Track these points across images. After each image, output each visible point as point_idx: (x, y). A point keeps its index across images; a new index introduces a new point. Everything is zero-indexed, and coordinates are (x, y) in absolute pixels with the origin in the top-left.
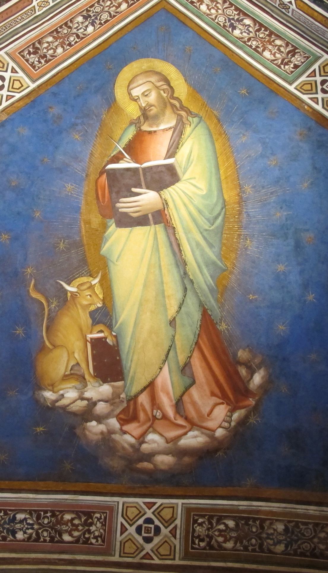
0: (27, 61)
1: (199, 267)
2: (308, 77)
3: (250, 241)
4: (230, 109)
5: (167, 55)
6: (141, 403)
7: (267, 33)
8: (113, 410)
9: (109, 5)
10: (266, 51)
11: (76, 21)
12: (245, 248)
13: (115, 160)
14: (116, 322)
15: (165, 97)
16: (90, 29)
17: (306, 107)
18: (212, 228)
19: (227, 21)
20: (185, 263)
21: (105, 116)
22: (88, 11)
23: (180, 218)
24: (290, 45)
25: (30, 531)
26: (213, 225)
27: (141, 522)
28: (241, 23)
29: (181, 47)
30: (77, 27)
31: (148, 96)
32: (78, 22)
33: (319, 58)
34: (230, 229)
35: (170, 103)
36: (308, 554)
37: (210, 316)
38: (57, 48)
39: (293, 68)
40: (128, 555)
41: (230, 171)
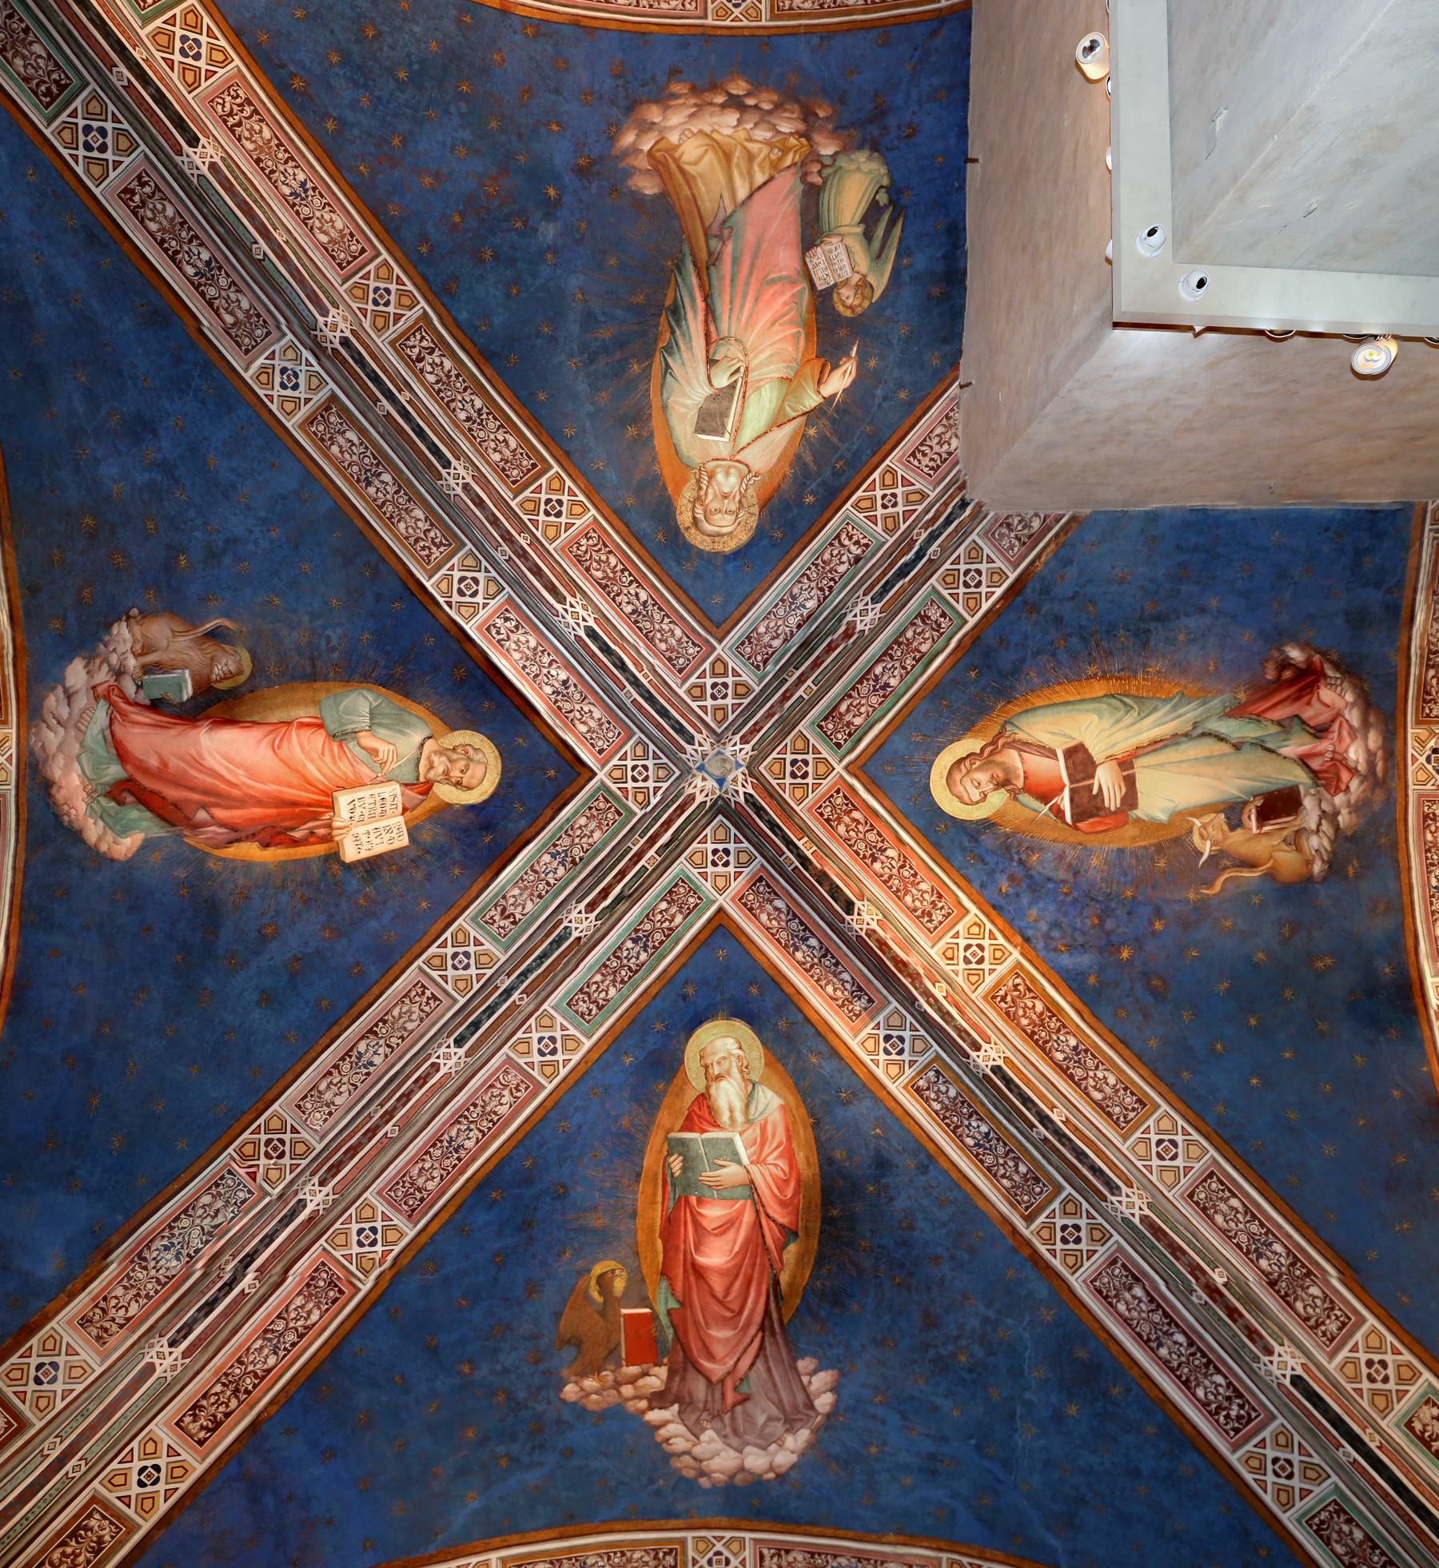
16: (891, 853)
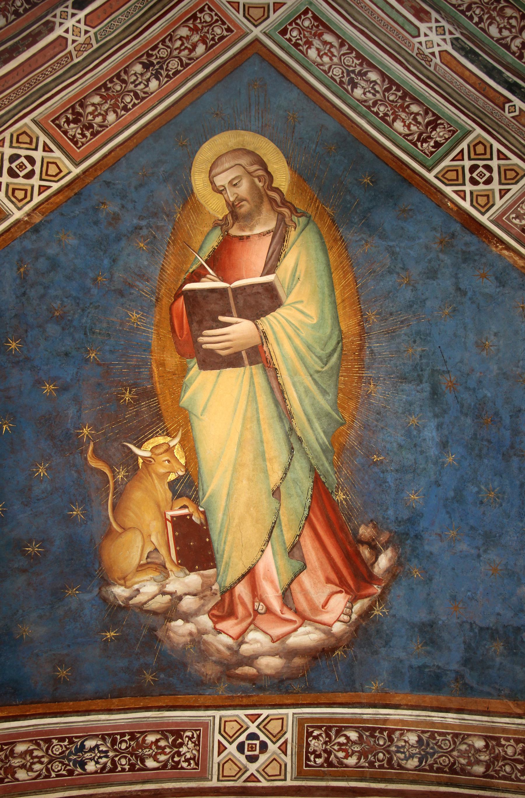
0: (65, 133)
1: (309, 420)
2: (453, 160)
3: (374, 385)
4: (349, 206)
5: (262, 126)
6: (239, 595)
7: (399, 94)
8: (203, 605)
9: (179, 46)
10: (397, 121)
11: (133, 72)
12: (367, 395)
13: (195, 277)
14: (204, 495)
15: (261, 188)
16: (154, 84)
17: (449, 204)
18: (326, 368)
19: (345, 75)
20: (290, 415)
21: (179, 215)
22: (149, 56)
23: (283, 356)
24: (430, 113)
25: (104, 760)
26: (326, 365)
27: (242, 738)
28: (364, 78)
29: (281, 112)
30: (135, 81)
31: (238, 185)
32: (136, 73)
33: (469, 133)
34: (347, 370)
35: (267, 195)
36: (447, 769)
37: (324, 483)
38: (107, 114)
39: (433, 147)
40: (229, 778)
41: (347, 292)
